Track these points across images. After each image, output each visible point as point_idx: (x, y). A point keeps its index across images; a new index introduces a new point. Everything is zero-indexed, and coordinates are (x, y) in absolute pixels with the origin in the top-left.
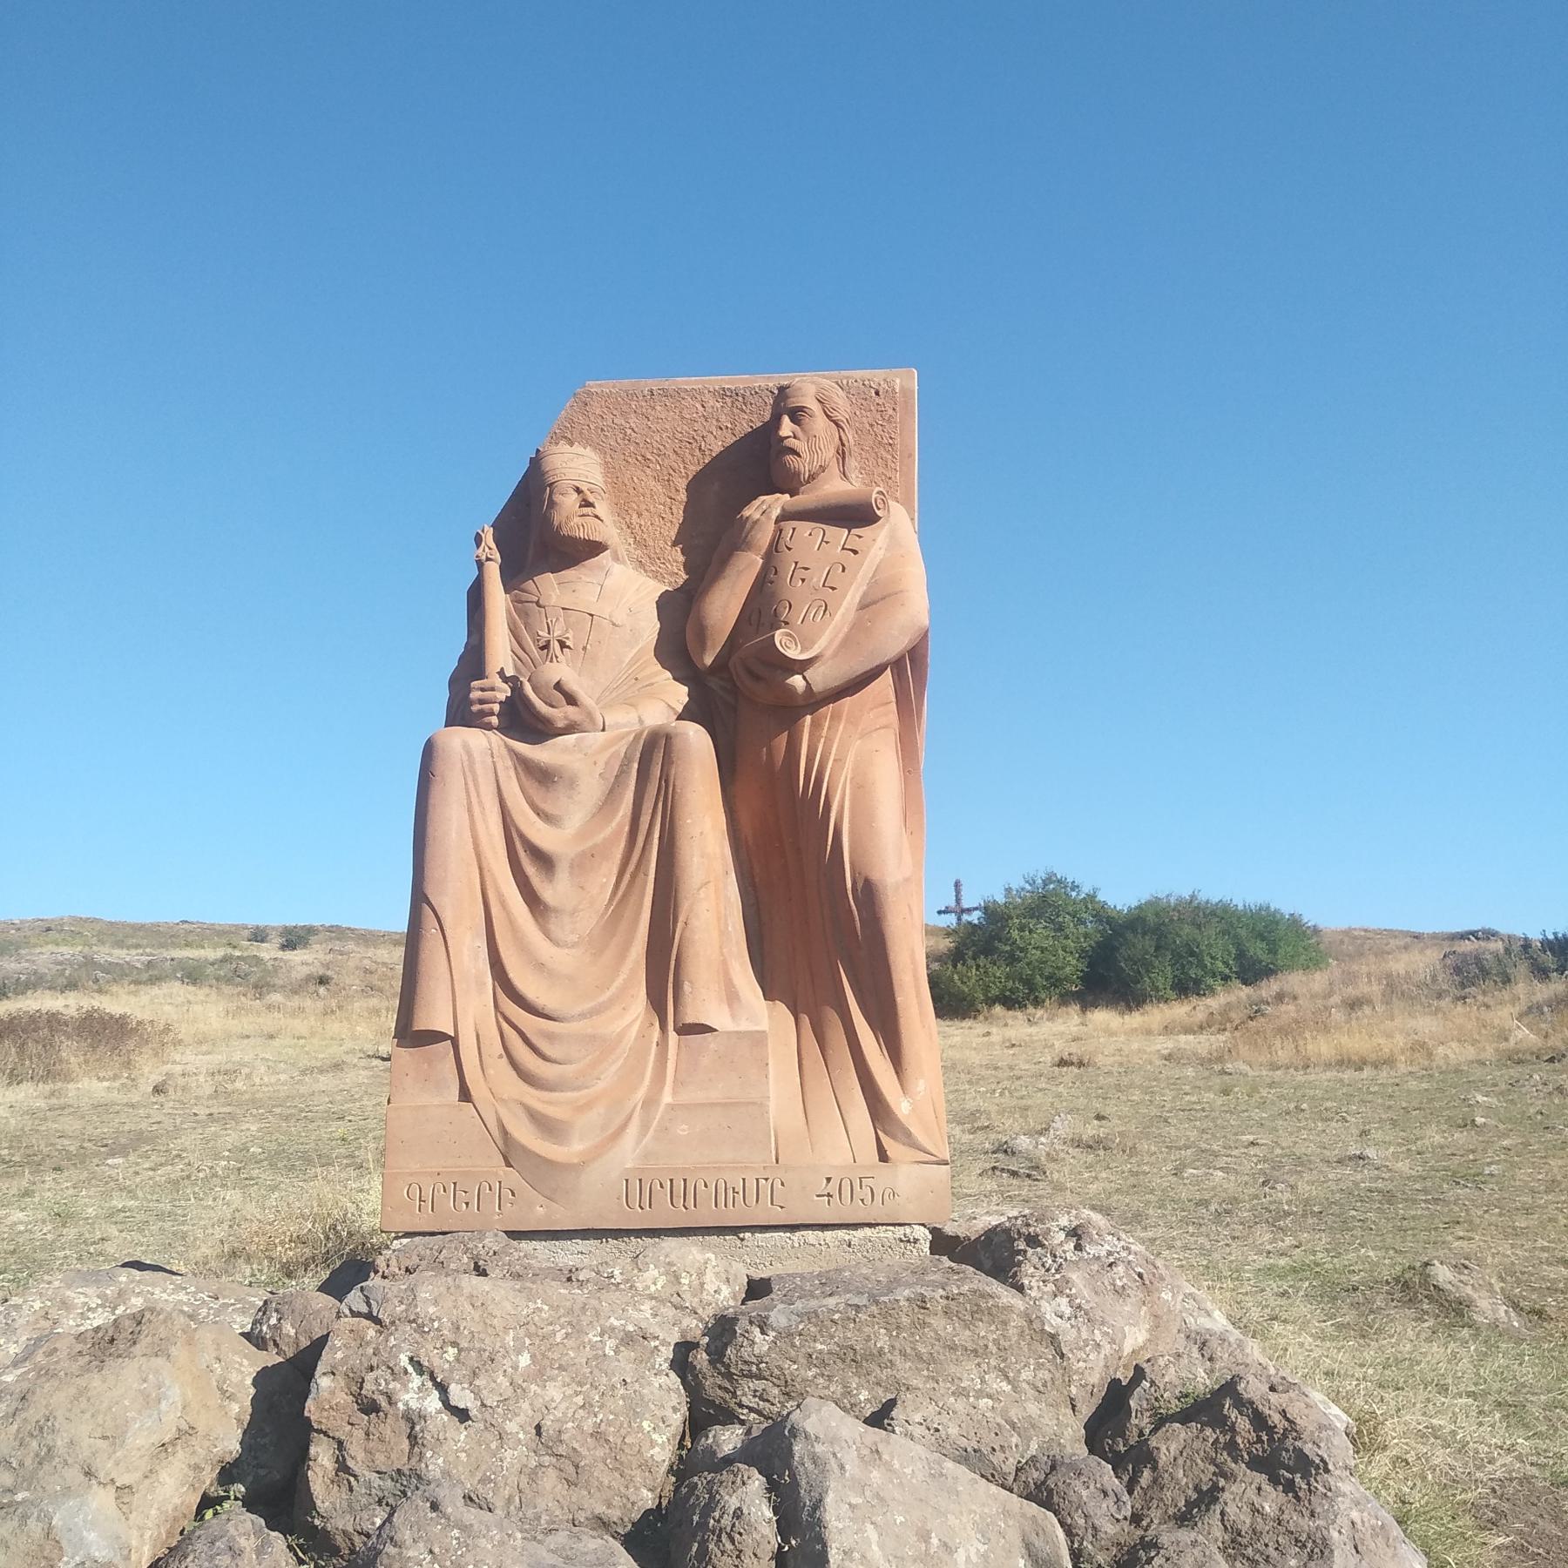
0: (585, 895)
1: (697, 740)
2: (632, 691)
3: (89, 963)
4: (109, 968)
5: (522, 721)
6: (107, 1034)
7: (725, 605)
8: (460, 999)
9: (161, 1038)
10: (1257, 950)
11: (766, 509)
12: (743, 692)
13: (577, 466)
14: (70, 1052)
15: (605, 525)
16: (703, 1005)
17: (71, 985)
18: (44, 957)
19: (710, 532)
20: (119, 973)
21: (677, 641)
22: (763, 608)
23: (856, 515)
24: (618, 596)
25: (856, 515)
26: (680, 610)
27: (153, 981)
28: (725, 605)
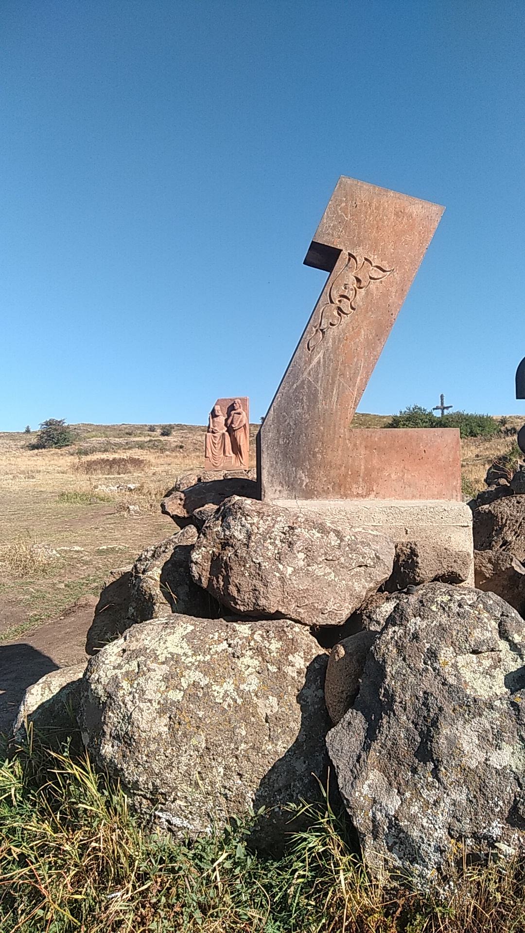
0: (218, 446)
1: (227, 434)
2: (223, 429)
3: (109, 443)
4: (115, 445)
5: (213, 432)
6: (137, 463)
7: (229, 421)
8: (209, 455)
9: (150, 464)
10: (477, 430)
11: (233, 412)
12: (231, 430)
13: (218, 408)
14: (130, 467)
15: (220, 413)
16: (227, 454)
17: (106, 451)
18: (95, 441)
19: (229, 415)
20: (119, 446)
21: (226, 425)
22: (232, 423)
23: (239, 414)
24: (222, 419)
25: (239, 414)
26: (226, 420)
27: (130, 448)
28: (229, 421)
